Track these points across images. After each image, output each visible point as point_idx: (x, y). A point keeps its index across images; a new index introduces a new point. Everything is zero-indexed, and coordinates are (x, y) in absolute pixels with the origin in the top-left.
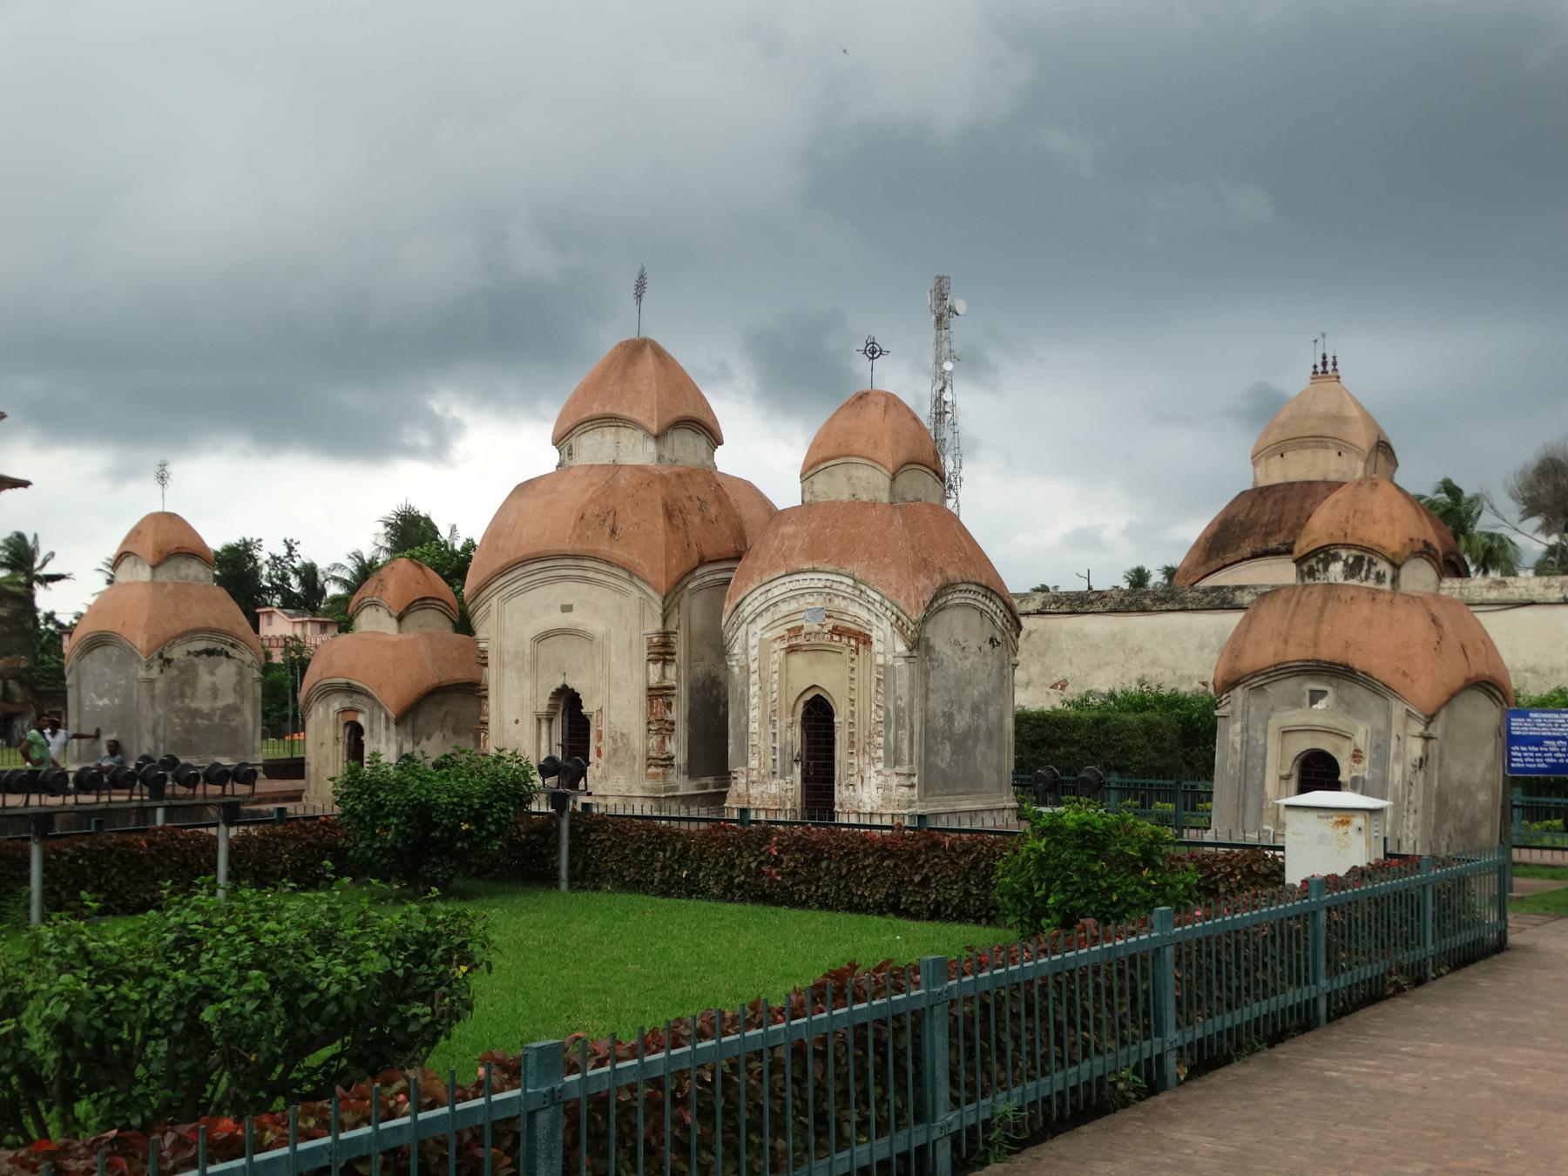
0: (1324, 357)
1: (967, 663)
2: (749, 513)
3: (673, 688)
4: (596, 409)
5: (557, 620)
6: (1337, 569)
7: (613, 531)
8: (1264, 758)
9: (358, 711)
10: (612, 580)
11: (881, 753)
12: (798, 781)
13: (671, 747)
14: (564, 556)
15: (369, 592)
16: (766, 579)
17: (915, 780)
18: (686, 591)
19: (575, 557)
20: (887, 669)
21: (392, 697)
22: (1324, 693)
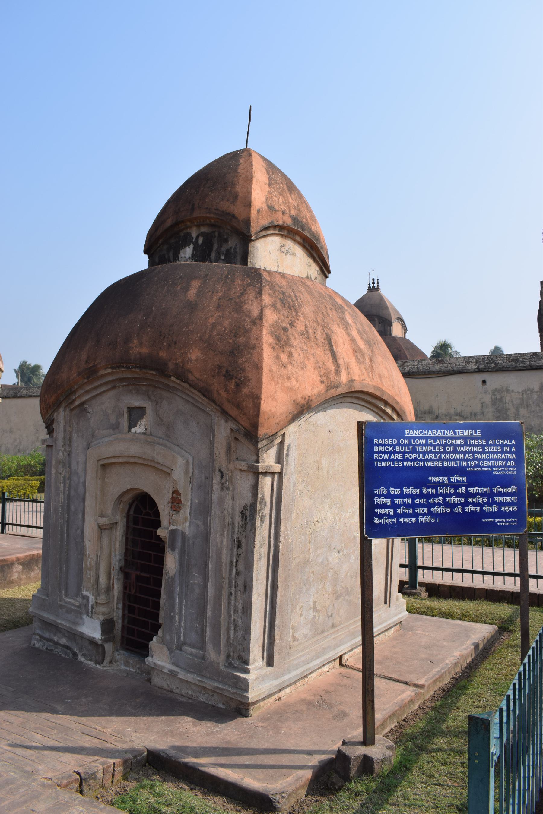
0: (373, 280)
8: (84, 500)
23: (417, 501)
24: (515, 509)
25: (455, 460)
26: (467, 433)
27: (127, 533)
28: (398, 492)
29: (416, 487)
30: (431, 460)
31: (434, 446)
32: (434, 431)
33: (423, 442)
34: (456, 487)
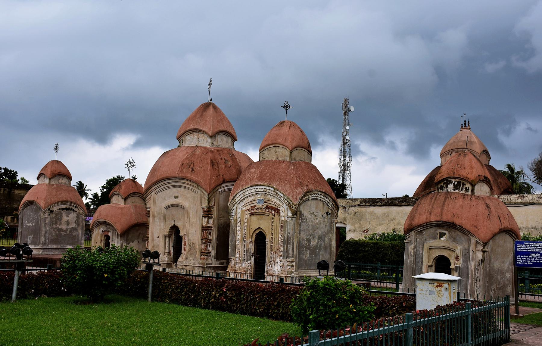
1: (317, 221)
2: (244, 165)
3: (211, 227)
4: (192, 127)
5: (173, 201)
6: (451, 186)
7: (193, 170)
8: (422, 258)
9: (109, 231)
10: (192, 187)
11: (282, 253)
12: (253, 263)
13: (210, 249)
14: (175, 178)
15: (116, 190)
16: (244, 188)
17: (294, 264)
18: (218, 192)
19: (180, 178)
20: (284, 222)
21: (119, 227)
22: (445, 234)
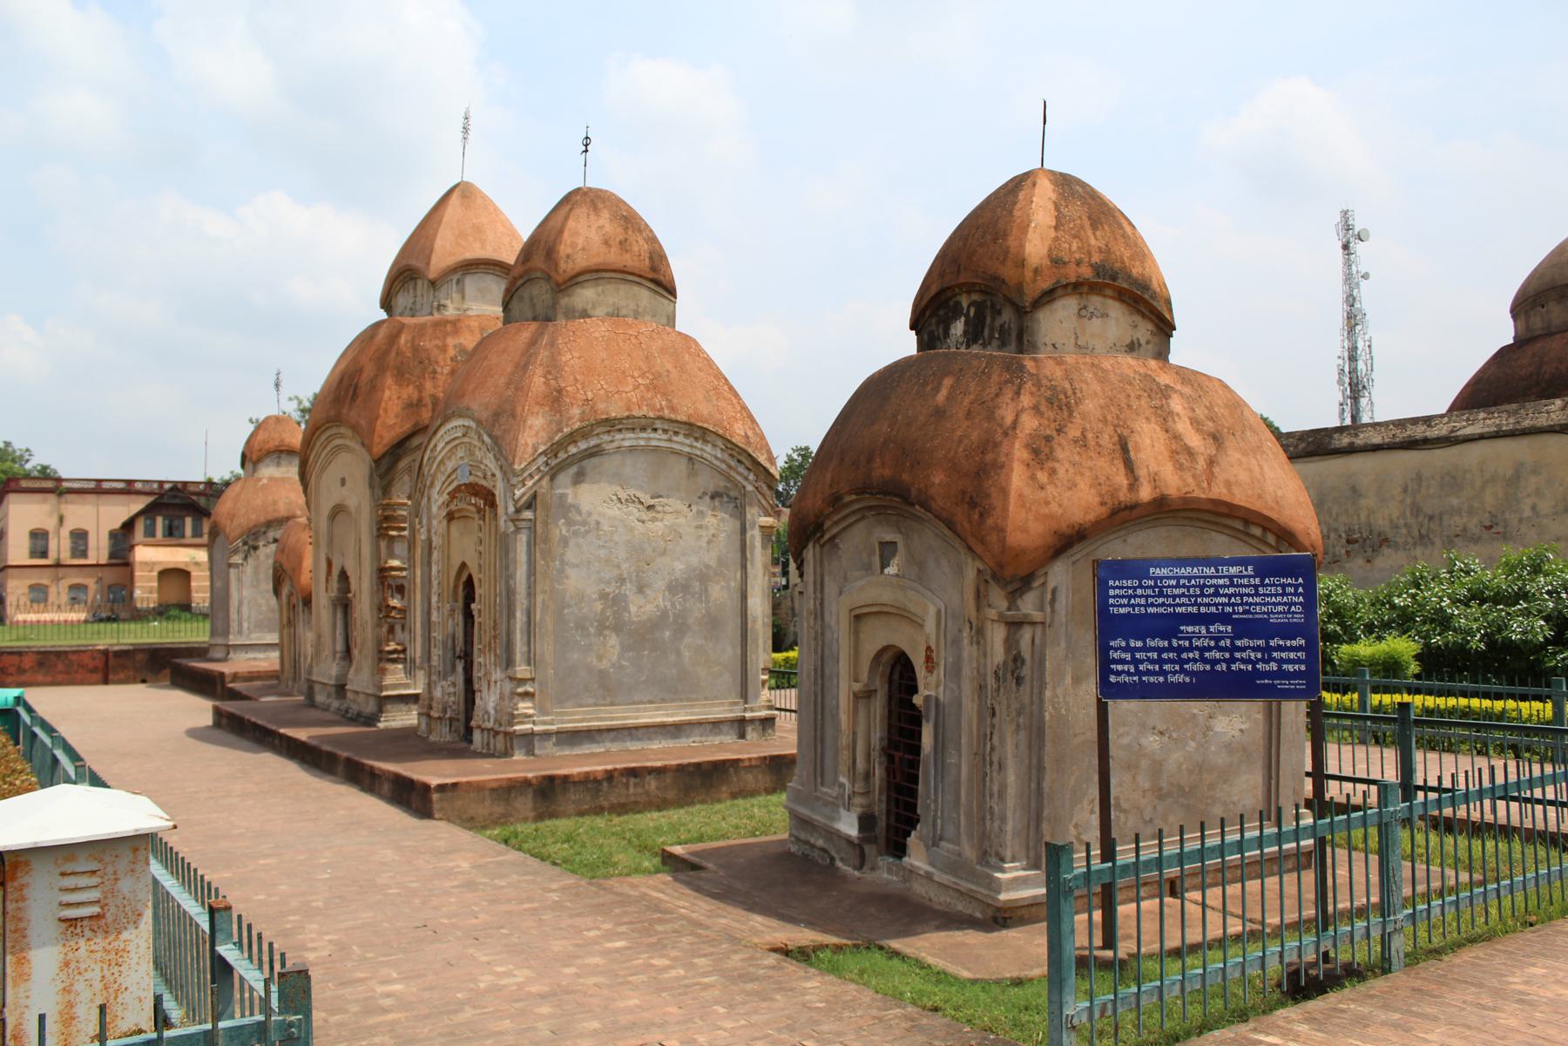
23: (1165, 656)
24: (1303, 668)
25: (1216, 605)
26: (1234, 570)
27: (889, 704)
28: (1139, 644)
29: (1163, 639)
30: (1183, 605)
31: (1188, 588)
32: (1189, 569)
33: (1173, 582)
34: (1217, 639)
